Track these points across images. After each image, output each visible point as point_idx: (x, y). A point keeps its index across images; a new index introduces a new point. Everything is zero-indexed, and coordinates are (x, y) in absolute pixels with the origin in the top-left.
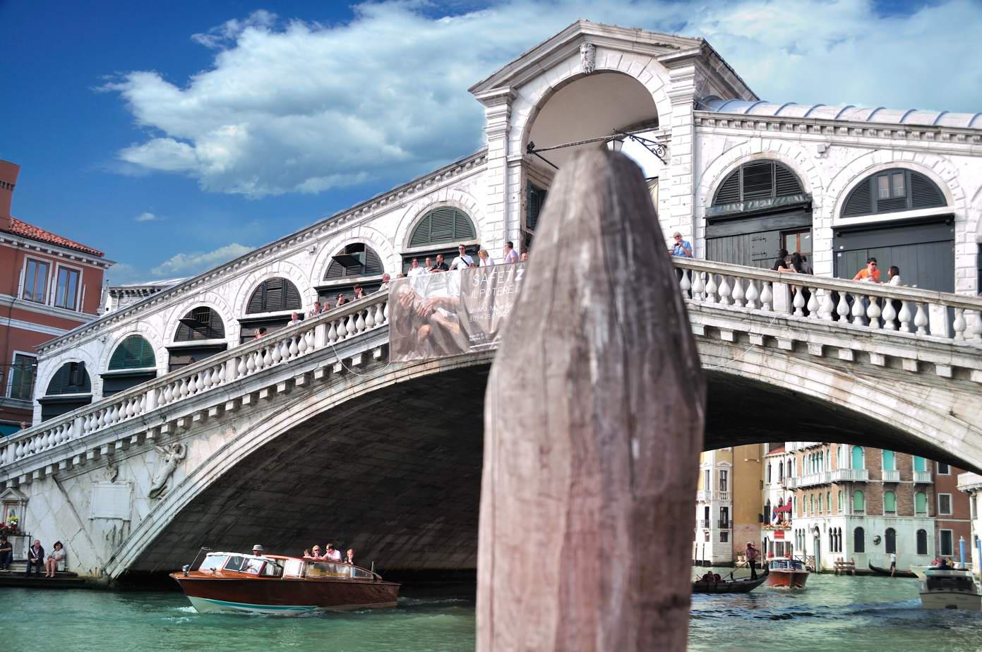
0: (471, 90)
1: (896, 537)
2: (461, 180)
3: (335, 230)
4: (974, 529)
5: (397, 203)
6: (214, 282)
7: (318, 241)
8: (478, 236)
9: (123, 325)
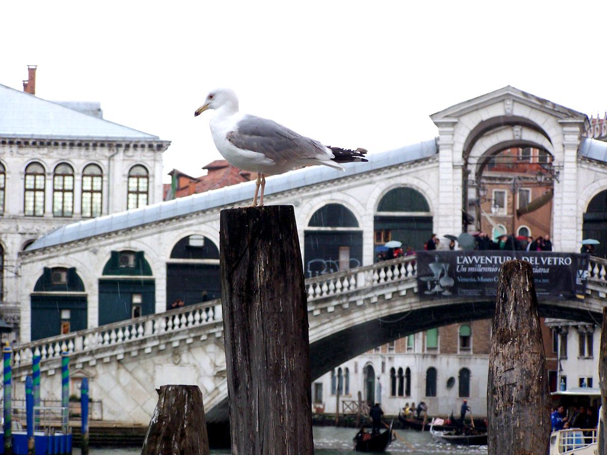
0: (431, 116)
1: (471, 378)
2: (417, 171)
3: (317, 192)
4: (561, 370)
5: (368, 180)
6: (207, 218)
7: (303, 198)
8: (431, 210)
9: (115, 243)
